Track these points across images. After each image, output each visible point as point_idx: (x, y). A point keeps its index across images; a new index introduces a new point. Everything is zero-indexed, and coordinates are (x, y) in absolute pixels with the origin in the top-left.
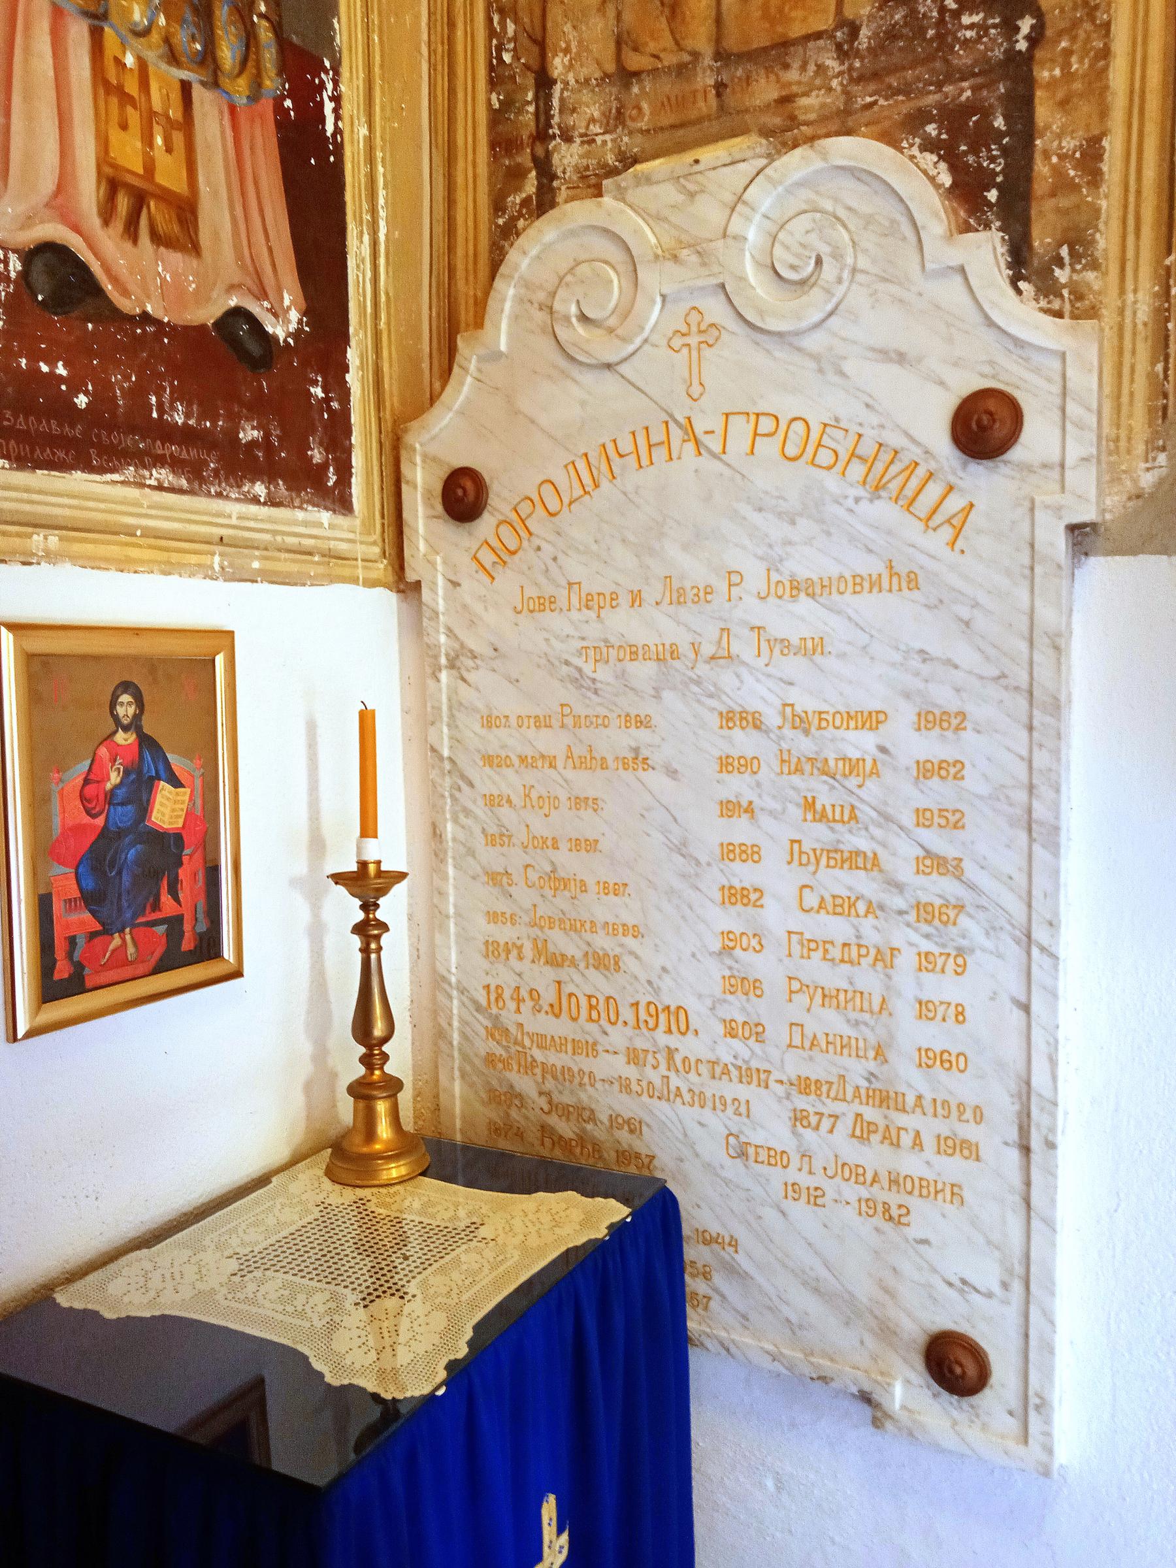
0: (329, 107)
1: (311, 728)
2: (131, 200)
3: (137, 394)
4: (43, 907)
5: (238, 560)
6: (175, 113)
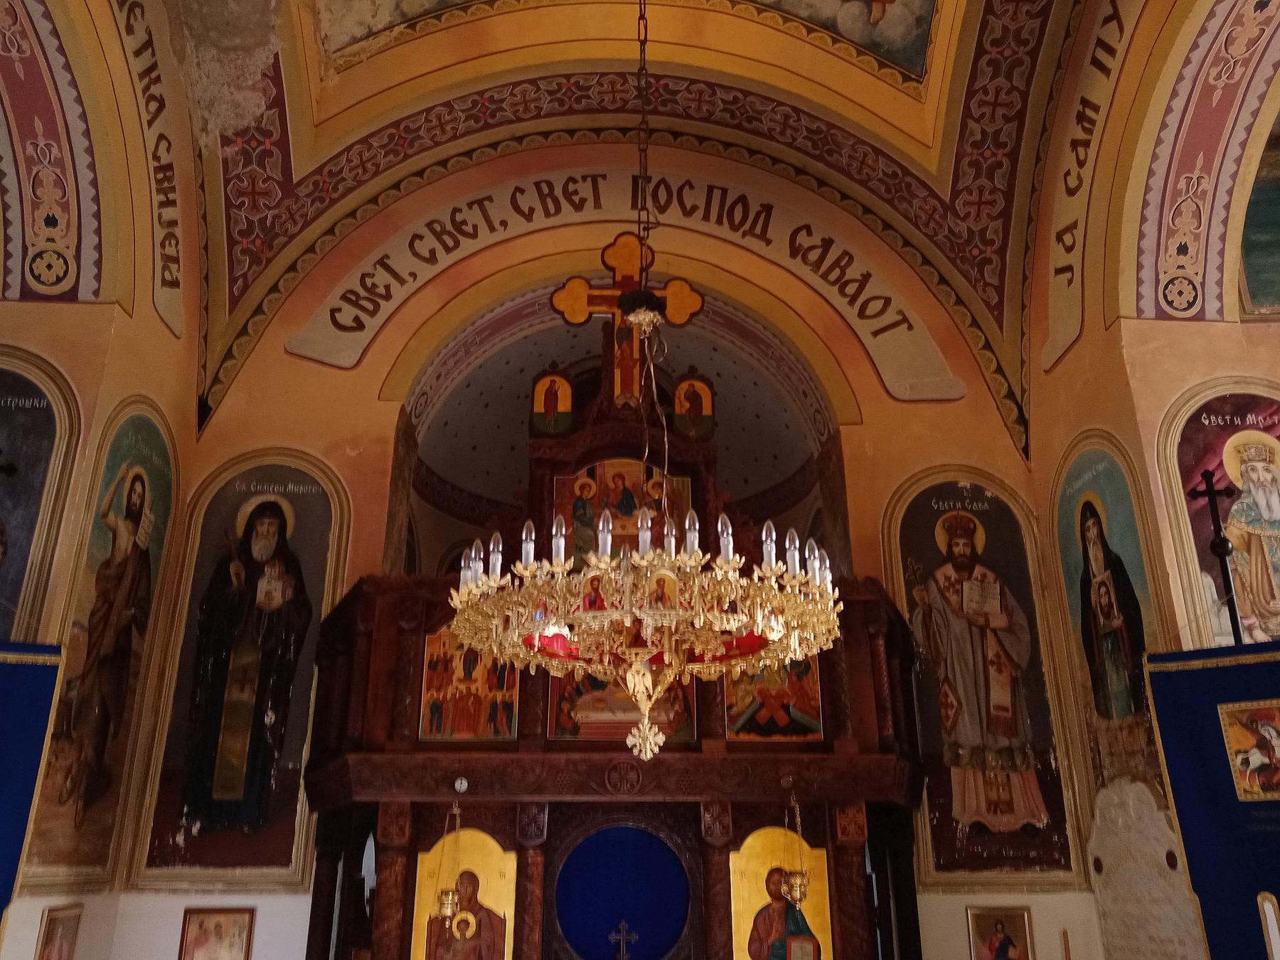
0: (1053, 762)
1: (1065, 934)
2: (993, 806)
5: (1032, 888)
6: (1005, 780)
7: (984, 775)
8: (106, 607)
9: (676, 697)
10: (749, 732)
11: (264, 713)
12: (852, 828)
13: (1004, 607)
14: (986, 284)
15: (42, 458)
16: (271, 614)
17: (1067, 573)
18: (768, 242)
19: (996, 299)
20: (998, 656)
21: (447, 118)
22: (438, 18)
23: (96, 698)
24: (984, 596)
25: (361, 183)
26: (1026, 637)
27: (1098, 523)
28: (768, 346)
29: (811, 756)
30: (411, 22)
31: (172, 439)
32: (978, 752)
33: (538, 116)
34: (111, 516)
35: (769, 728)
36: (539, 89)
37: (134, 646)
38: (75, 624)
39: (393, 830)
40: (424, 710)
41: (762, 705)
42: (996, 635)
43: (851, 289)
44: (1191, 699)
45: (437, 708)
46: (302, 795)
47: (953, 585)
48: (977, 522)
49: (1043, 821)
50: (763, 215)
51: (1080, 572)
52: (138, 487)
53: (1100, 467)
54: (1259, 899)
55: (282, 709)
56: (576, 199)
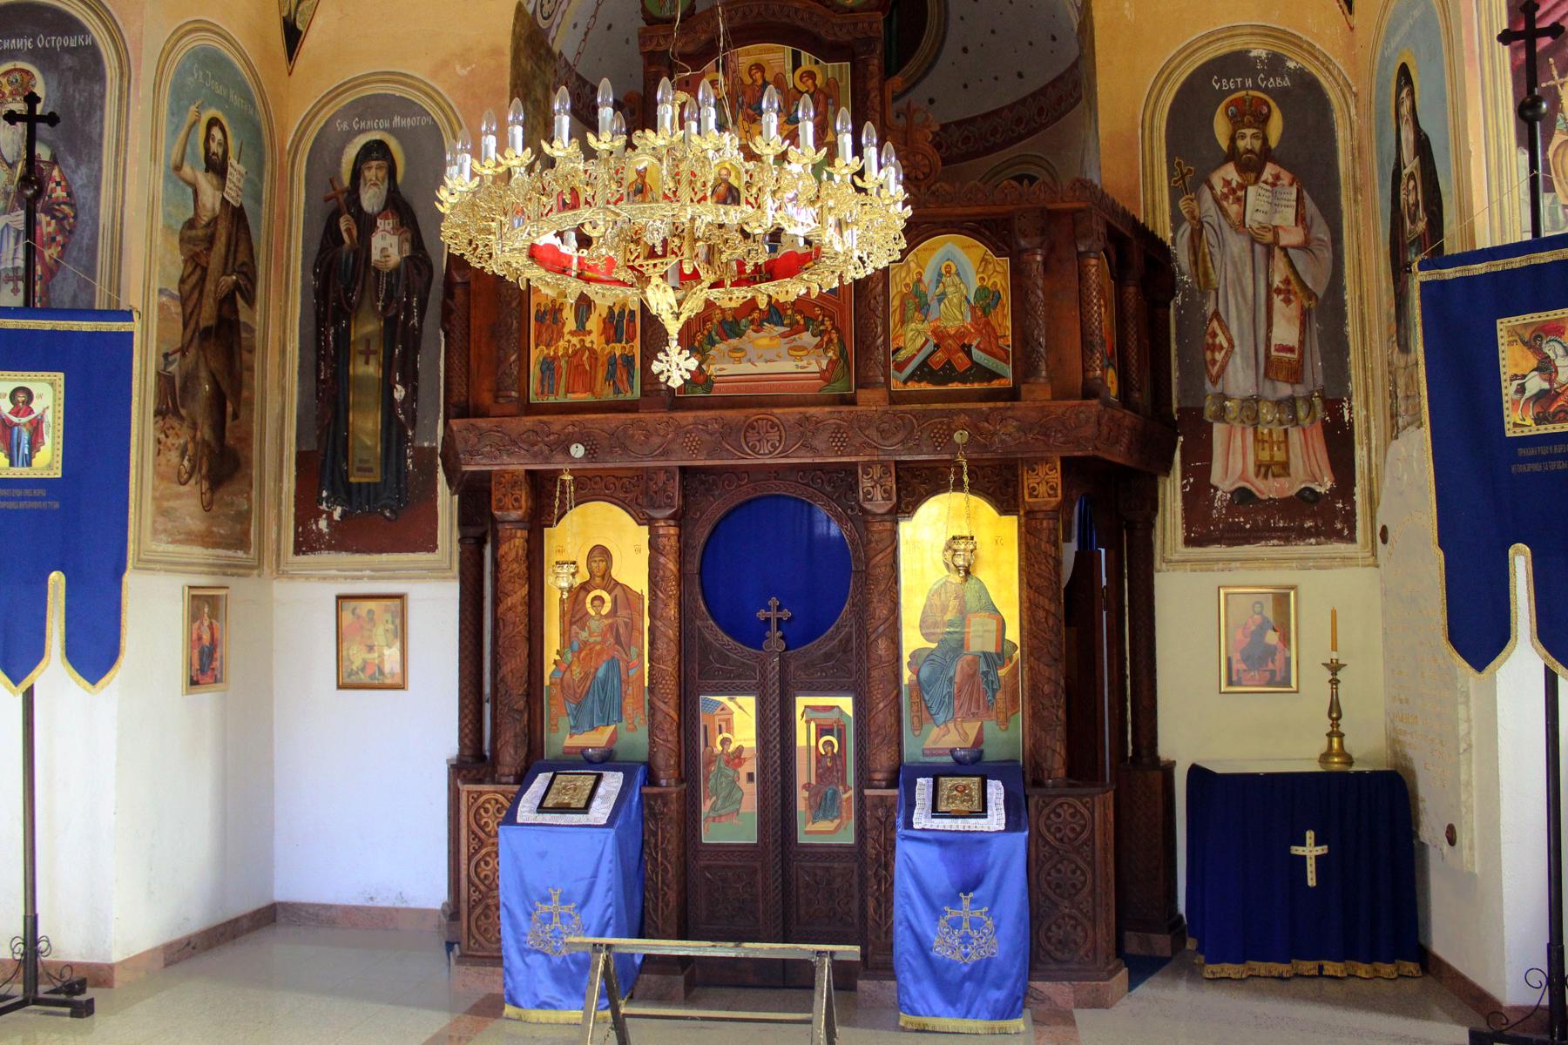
2: (1264, 469)
3: (1267, 521)
4: (1229, 660)
5: (1303, 563)
7: (1255, 430)
8: (198, 272)
9: (830, 340)
10: (919, 381)
11: (391, 389)
12: (1042, 489)
13: (1300, 218)
15: (94, 106)
16: (389, 275)
17: (1381, 166)
20: (1287, 281)
23: (203, 374)
24: (1275, 205)
26: (1327, 255)
27: (1412, 93)
29: (991, 405)
31: (255, 75)
32: (1251, 405)
34: (187, 170)
35: (947, 373)
37: (243, 318)
38: (161, 291)
39: (508, 501)
40: (534, 370)
41: (937, 346)
42: (1287, 255)
44: (1465, 312)
45: (549, 365)
46: (441, 476)
47: (1234, 191)
48: (1273, 104)
49: (1325, 484)
51: (1393, 162)
52: (216, 132)
53: (1416, 13)
54: (1511, 551)
55: (411, 380)
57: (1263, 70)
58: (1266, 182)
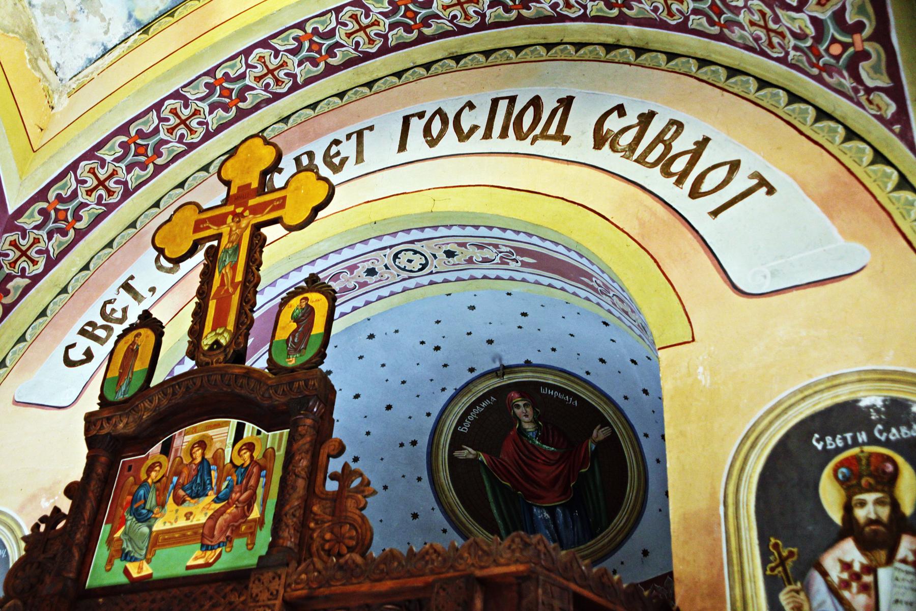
14: (869, 91)
18: (565, 140)
19: (893, 108)
21: (186, 112)
22: (172, 15)
25: (111, 208)
28: (590, 277)
30: (145, 28)
33: (295, 87)
36: (277, 53)
43: (678, 166)
47: (856, 577)
50: (560, 111)
56: (336, 161)
57: (880, 421)
58: (904, 561)
